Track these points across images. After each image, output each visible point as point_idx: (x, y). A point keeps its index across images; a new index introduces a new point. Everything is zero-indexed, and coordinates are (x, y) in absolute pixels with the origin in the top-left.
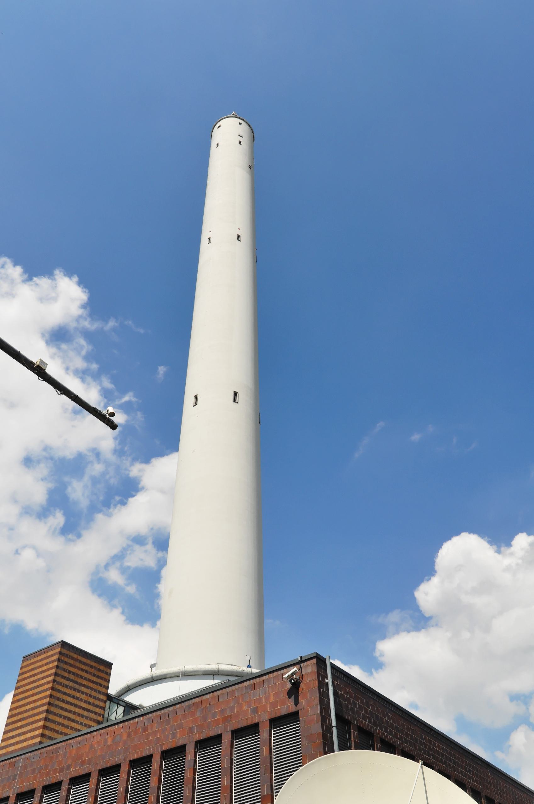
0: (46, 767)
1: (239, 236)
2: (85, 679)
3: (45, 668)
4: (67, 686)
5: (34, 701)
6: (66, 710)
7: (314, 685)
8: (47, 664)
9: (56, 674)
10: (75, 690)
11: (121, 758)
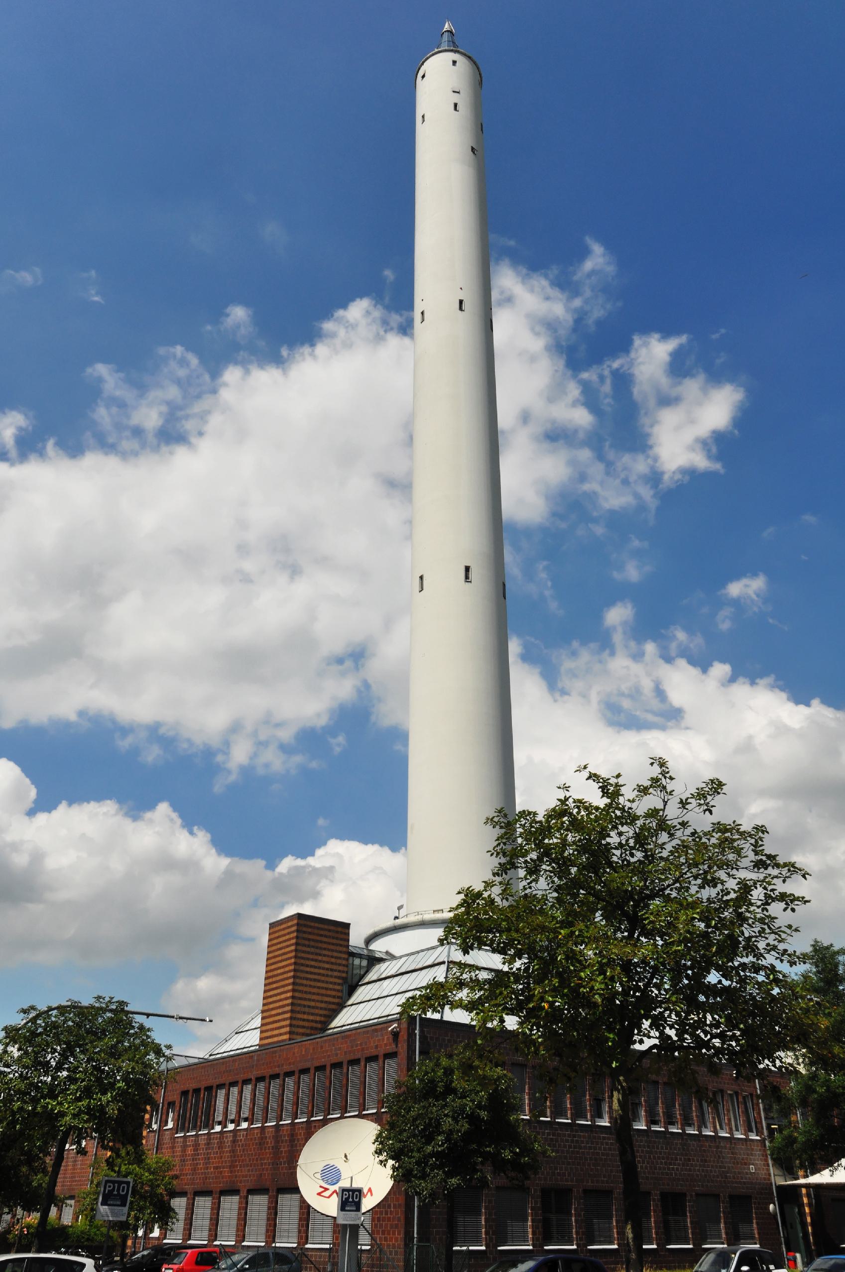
2: (325, 943)
3: (287, 937)
4: (308, 953)
5: (283, 967)
7: (406, 1038)
8: (289, 933)
9: (297, 944)
10: (317, 954)
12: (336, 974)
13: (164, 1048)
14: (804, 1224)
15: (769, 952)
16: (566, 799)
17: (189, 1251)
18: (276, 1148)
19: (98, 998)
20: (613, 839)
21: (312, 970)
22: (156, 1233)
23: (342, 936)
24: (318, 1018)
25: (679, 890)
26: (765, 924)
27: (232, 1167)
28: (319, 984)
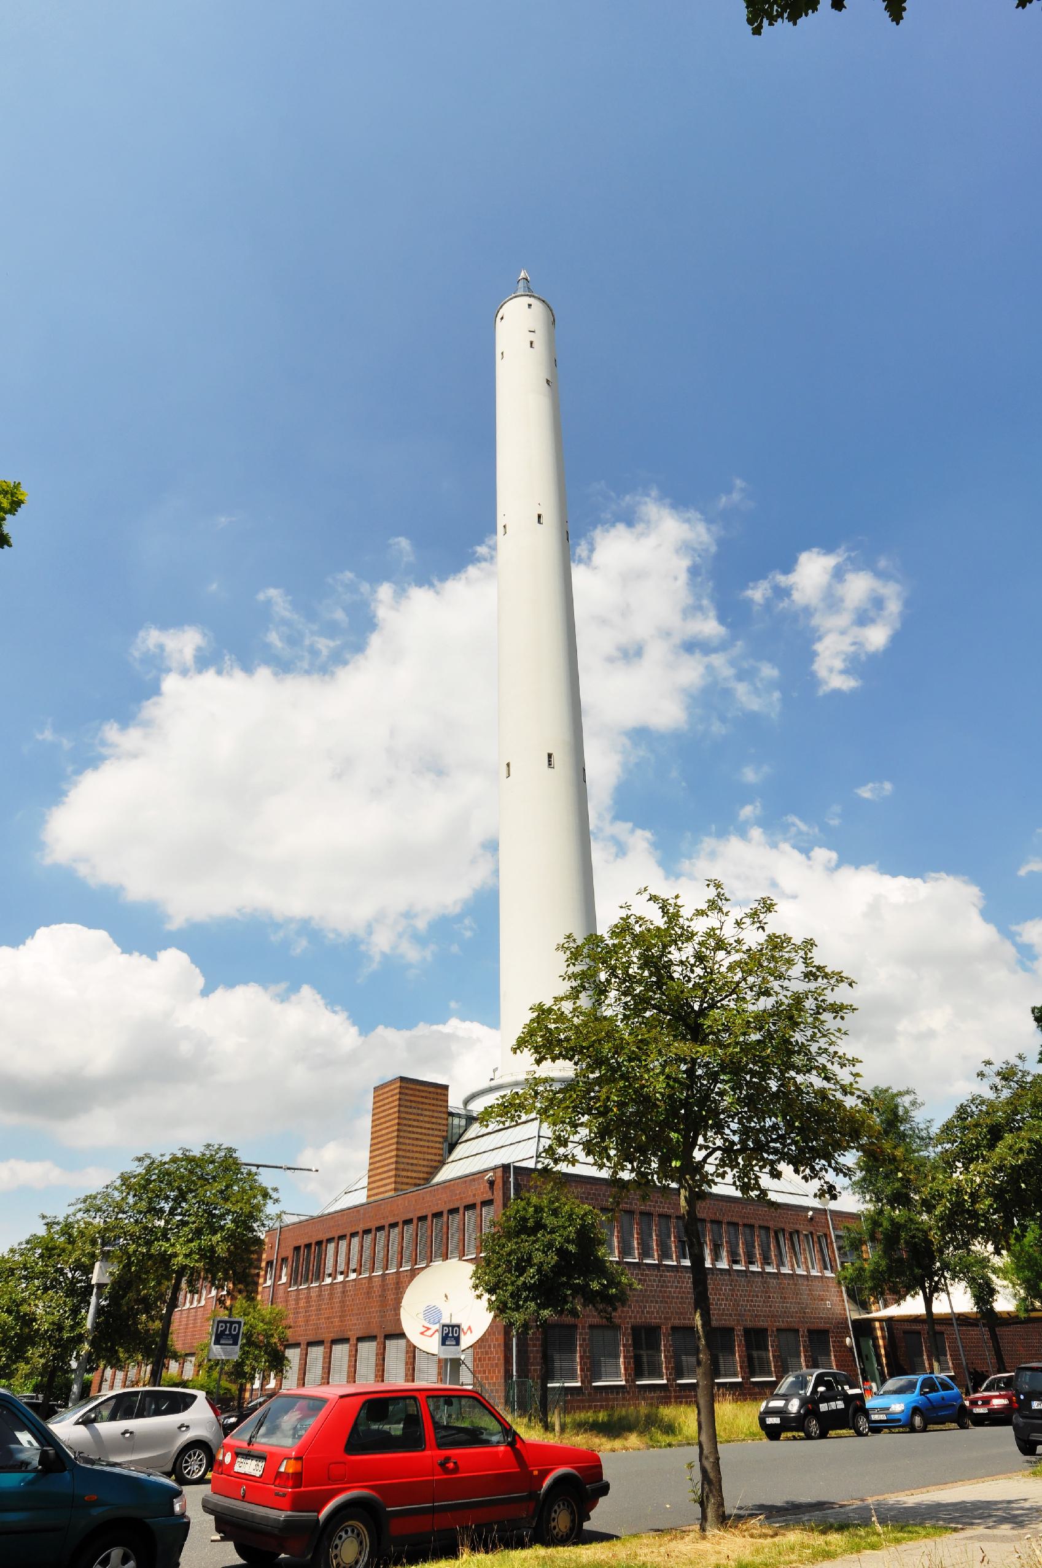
3: (391, 1099)
7: (501, 1185)
9: (399, 1105)
12: (436, 1133)
13: (270, 1191)
14: (878, 1356)
15: (820, 1054)
16: (628, 917)
18: (383, 1296)
19: (208, 1146)
20: (675, 955)
21: (415, 1130)
22: (272, 1384)
23: (442, 1097)
24: (422, 1175)
25: (736, 1000)
26: (816, 1027)
27: (342, 1317)
28: (422, 1143)
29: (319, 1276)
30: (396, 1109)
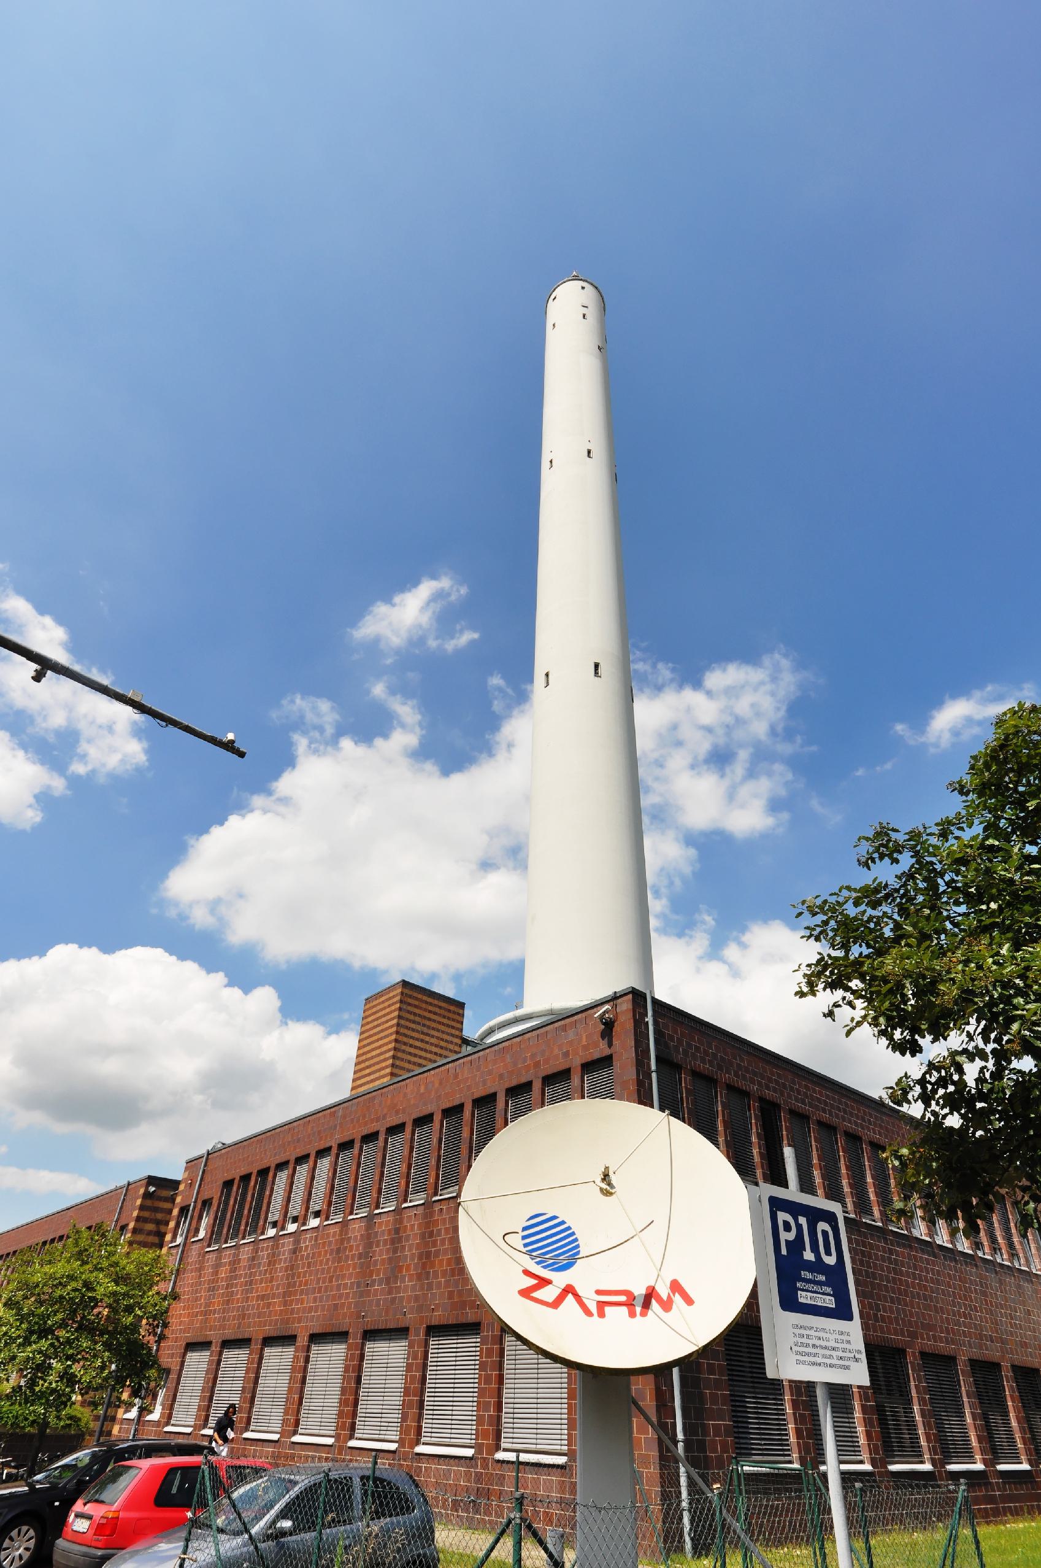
0: (364, 1117)
1: (589, 452)
2: (434, 1021)
3: (388, 1010)
4: (413, 1030)
5: (380, 1047)
6: (415, 1055)
7: (630, 1026)
8: (389, 1006)
9: (399, 1017)
10: (423, 1033)
11: (434, 1107)
17: (146, 1464)
29: (255, 1227)
30: (395, 1021)
